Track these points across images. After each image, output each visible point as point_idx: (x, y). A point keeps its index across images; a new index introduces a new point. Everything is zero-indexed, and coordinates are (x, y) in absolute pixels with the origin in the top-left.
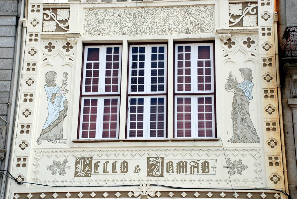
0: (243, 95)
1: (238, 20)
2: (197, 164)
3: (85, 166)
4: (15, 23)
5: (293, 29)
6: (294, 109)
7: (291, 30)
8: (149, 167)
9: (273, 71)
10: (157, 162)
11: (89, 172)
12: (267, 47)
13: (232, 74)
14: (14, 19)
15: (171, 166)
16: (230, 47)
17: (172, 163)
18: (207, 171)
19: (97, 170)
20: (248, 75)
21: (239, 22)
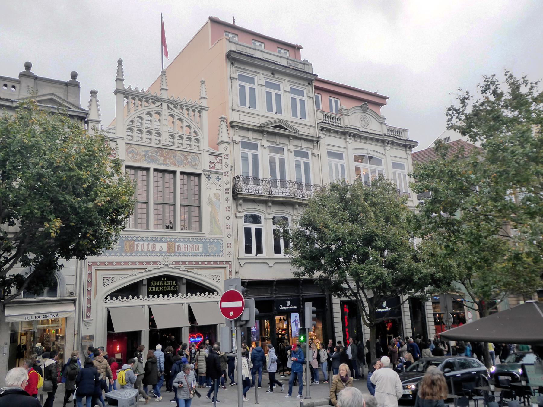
1: (213, 165)
3: (130, 246)
8: (167, 247)
12: (227, 183)
16: (209, 180)
20: (217, 197)
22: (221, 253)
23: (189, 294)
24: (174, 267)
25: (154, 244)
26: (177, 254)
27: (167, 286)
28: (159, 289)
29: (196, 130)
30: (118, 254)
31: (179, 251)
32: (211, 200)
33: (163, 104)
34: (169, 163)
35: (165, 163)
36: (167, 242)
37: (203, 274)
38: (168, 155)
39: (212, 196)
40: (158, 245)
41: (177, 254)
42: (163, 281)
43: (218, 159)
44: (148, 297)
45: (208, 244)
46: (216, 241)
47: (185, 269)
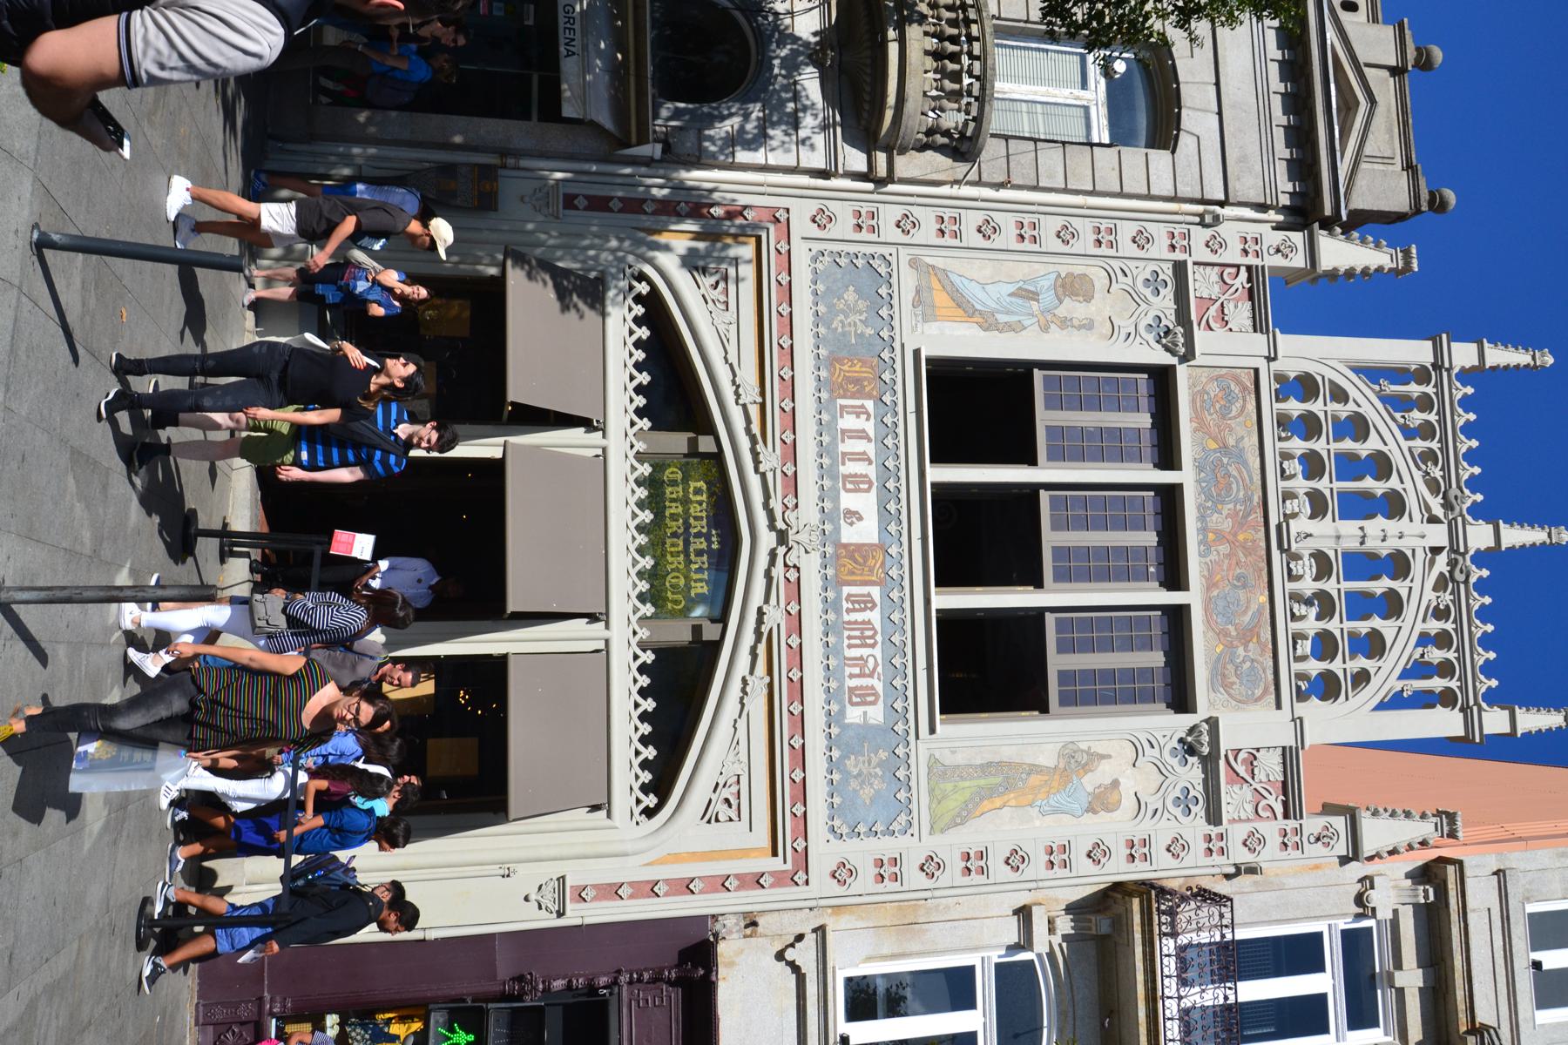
0: (1053, 791)
1: (1241, 770)
2: (871, 675)
3: (857, 381)
4: (1208, 196)
5: (1228, 915)
6: (1019, 920)
7: (1224, 909)
8: (859, 547)
9: (1119, 870)
10: (871, 570)
11: (841, 391)
13: (1103, 761)
14: (1221, 197)
15: (863, 606)
17: (872, 609)
18: (855, 699)
19: (848, 413)
20: (1103, 801)
21: (1238, 775)
22: (845, 830)
23: (648, 657)
24: (774, 573)
25: (870, 483)
26: (831, 595)
27: (686, 552)
28: (674, 517)
29: (1375, 682)
30: (822, 330)
31: (845, 605)
32: (1086, 768)
33: (1443, 528)
34: (1213, 557)
35: (1211, 536)
36: (882, 548)
37: (742, 724)
38: (1248, 552)
39: (1102, 774)
40: (865, 503)
41: (831, 595)
42: (708, 537)
43: (1271, 800)
44: (640, 457)
45: (883, 755)
46: (902, 795)
47: (765, 629)
